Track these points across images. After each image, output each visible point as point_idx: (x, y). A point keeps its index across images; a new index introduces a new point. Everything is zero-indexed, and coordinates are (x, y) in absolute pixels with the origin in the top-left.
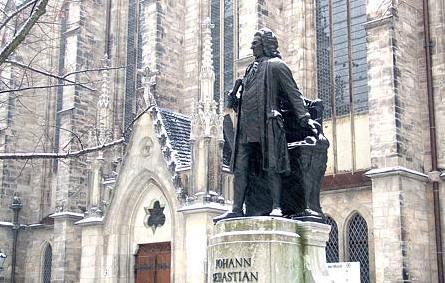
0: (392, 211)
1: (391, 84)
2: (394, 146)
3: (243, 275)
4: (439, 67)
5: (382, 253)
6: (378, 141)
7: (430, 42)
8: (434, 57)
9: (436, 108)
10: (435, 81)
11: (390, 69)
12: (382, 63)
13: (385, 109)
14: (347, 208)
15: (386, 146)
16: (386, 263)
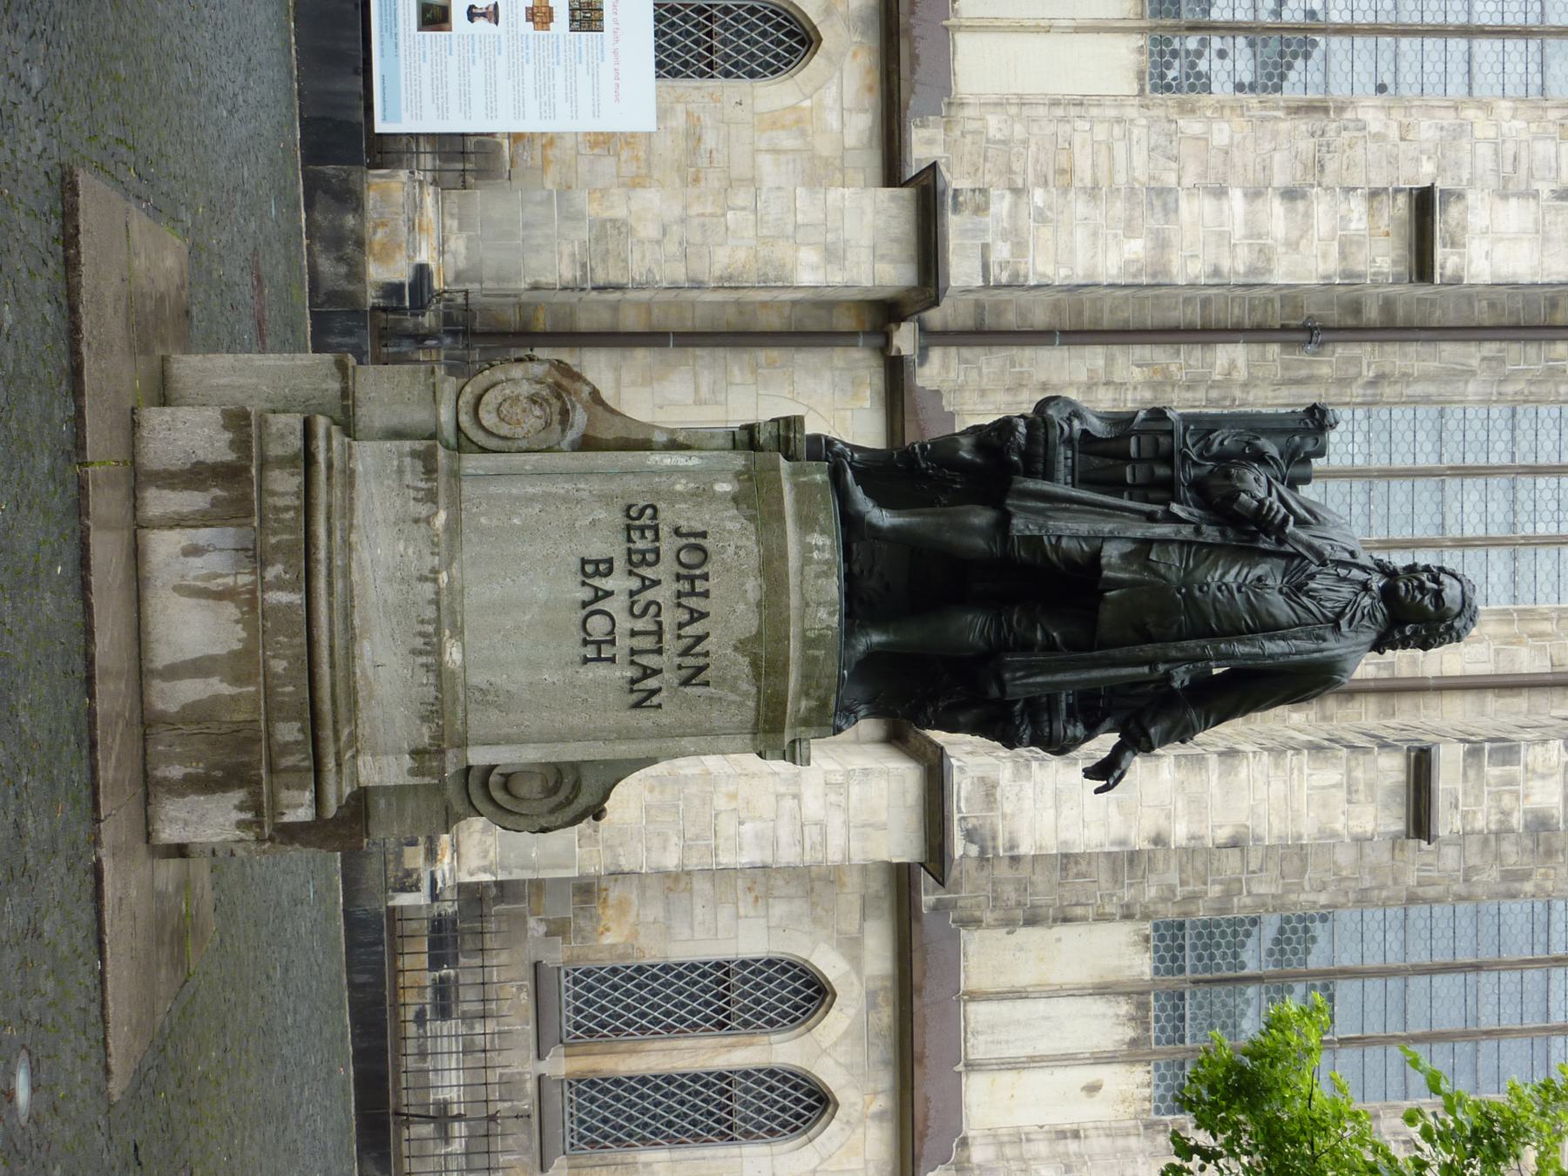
0: (809, 256)
1: (1217, 272)
2: (1016, 275)
3: (650, 661)
4: (1241, 362)
5: (677, 211)
6: (1041, 217)
7: (1322, 344)
8: (1274, 350)
9: (1116, 349)
10: (1197, 351)
11: (1270, 271)
12: (1292, 245)
13: (1136, 248)
14: (828, 11)
15: (1020, 246)
16: (649, 231)
